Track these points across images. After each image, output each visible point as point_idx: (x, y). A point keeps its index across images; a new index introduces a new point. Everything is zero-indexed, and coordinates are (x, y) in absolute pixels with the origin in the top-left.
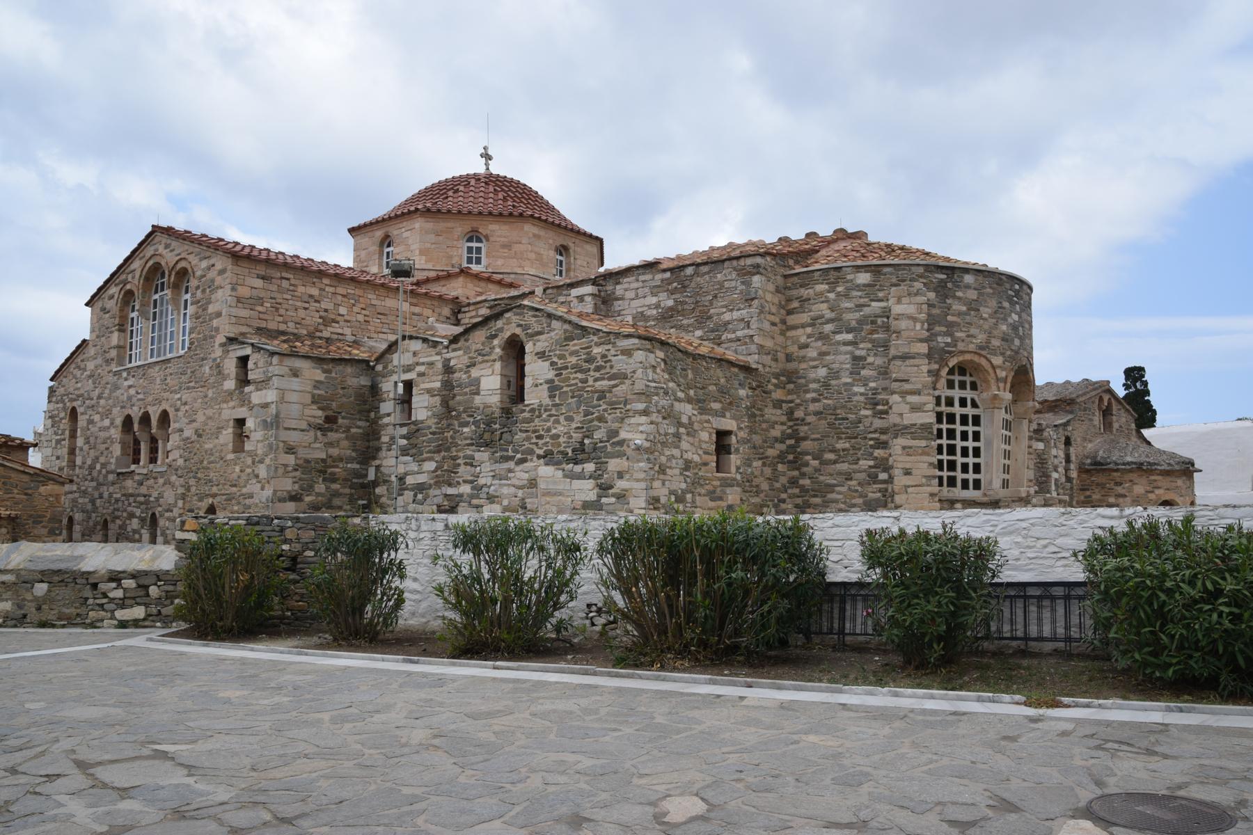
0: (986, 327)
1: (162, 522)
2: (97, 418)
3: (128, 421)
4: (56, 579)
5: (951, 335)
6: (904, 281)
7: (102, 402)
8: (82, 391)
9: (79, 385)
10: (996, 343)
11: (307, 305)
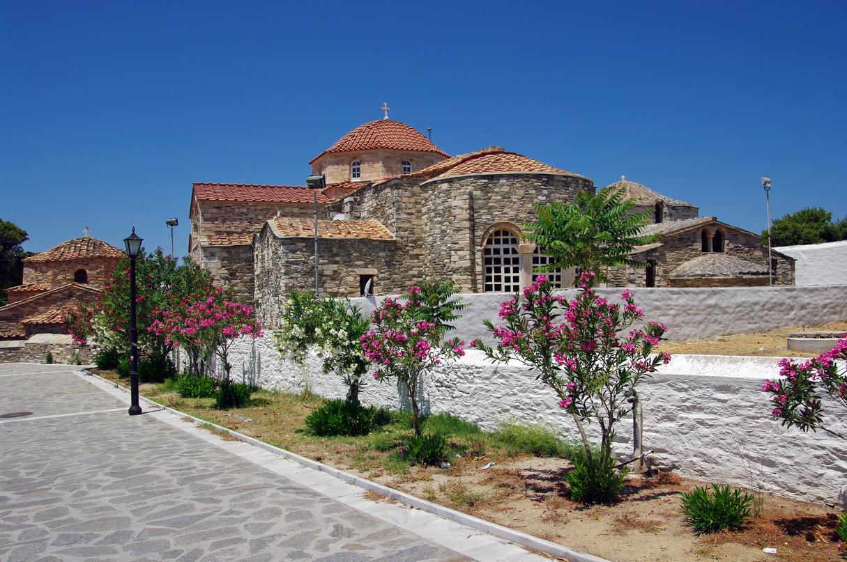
0: (515, 206)
10: (522, 216)
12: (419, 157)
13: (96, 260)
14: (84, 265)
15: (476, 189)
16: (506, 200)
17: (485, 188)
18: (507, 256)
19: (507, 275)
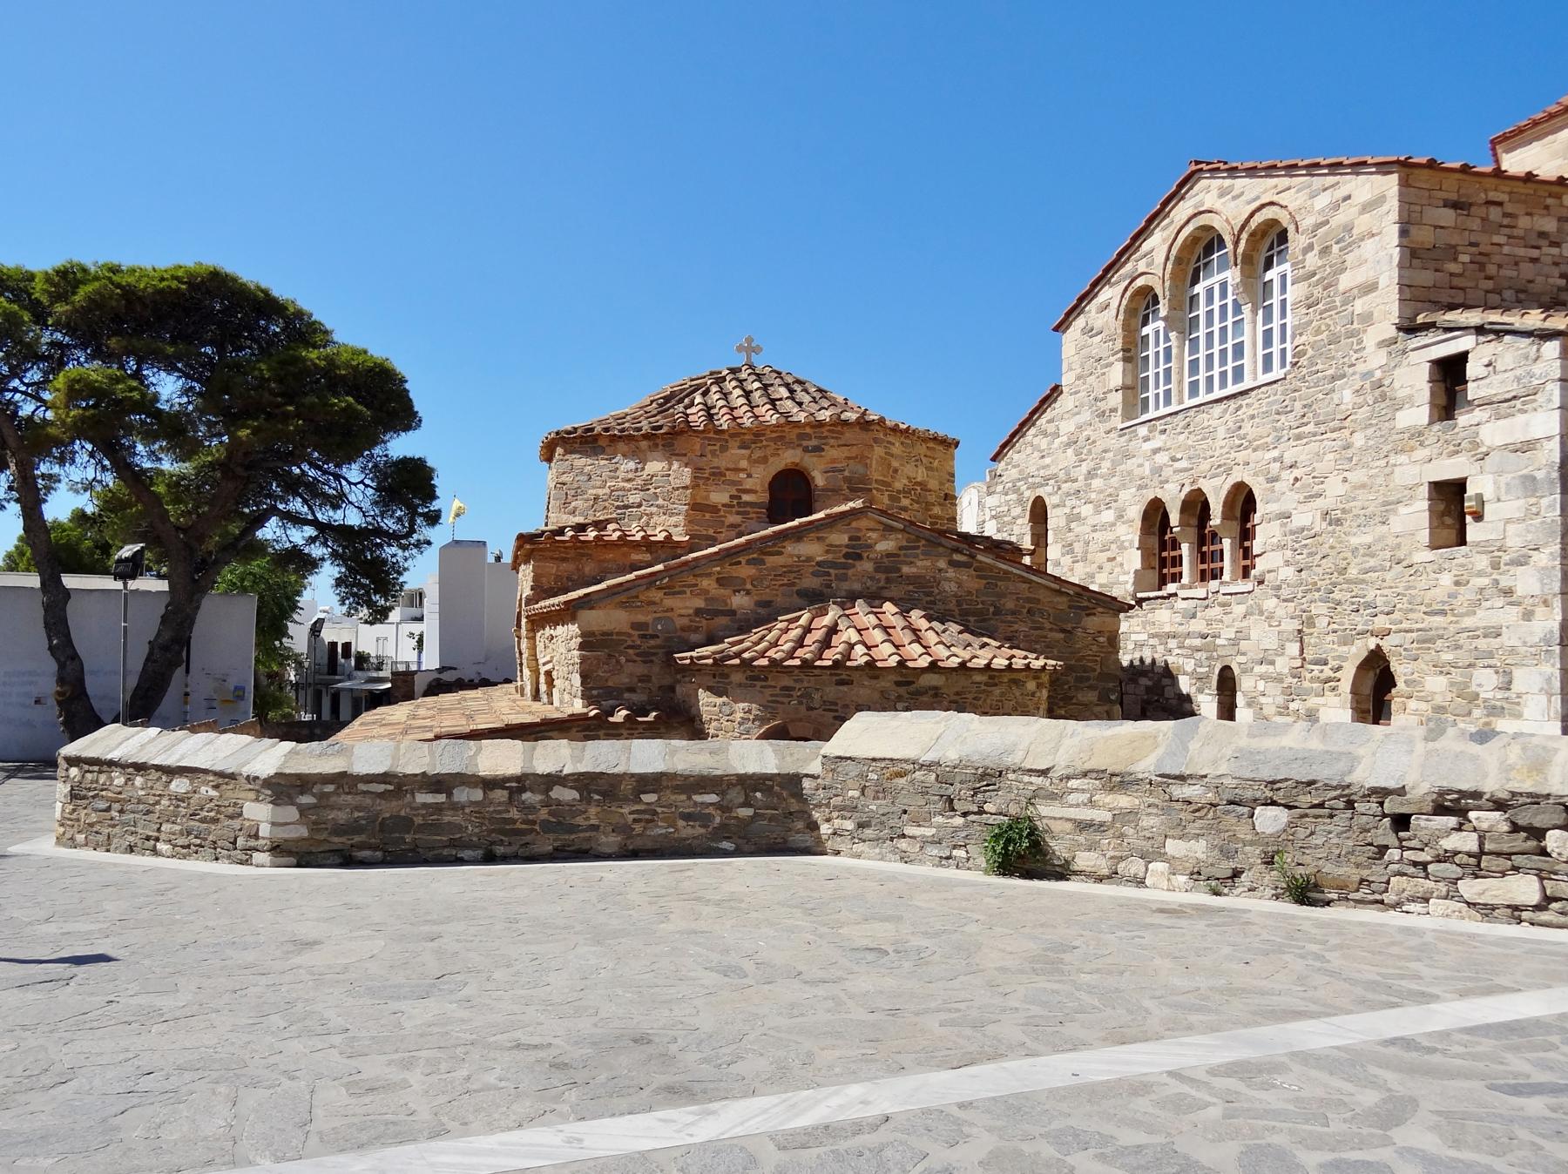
1: (1245, 684)
2: (1086, 510)
3: (1155, 514)
4: (1305, 800)
7: (1097, 483)
8: (1053, 470)
9: (1047, 461)
11: (1535, 253)
13: (849, 435)
14: (806, 450)
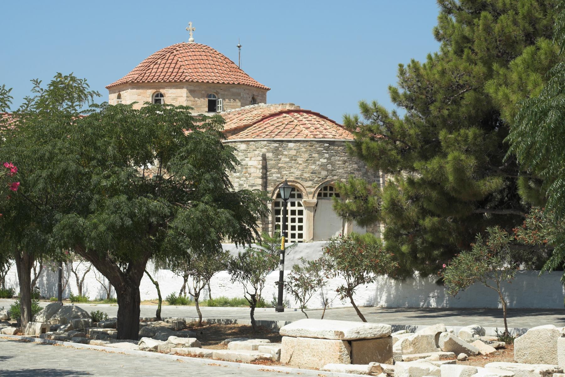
0: (301, 167)
5: (280, 173)
6: (258, 148)
10: (306, 175)
12: (225, 91)
15: (268, 151)
16: (293, 162)
17: (276, 152)
18: (293, 208)
19: (293, 224)
